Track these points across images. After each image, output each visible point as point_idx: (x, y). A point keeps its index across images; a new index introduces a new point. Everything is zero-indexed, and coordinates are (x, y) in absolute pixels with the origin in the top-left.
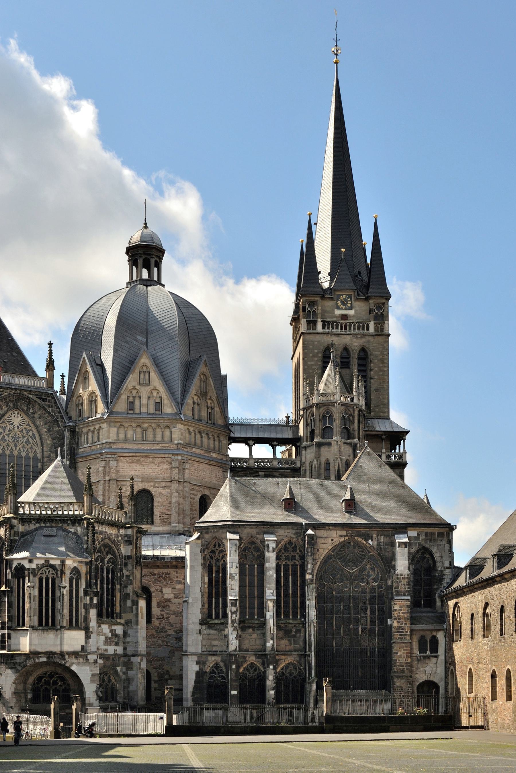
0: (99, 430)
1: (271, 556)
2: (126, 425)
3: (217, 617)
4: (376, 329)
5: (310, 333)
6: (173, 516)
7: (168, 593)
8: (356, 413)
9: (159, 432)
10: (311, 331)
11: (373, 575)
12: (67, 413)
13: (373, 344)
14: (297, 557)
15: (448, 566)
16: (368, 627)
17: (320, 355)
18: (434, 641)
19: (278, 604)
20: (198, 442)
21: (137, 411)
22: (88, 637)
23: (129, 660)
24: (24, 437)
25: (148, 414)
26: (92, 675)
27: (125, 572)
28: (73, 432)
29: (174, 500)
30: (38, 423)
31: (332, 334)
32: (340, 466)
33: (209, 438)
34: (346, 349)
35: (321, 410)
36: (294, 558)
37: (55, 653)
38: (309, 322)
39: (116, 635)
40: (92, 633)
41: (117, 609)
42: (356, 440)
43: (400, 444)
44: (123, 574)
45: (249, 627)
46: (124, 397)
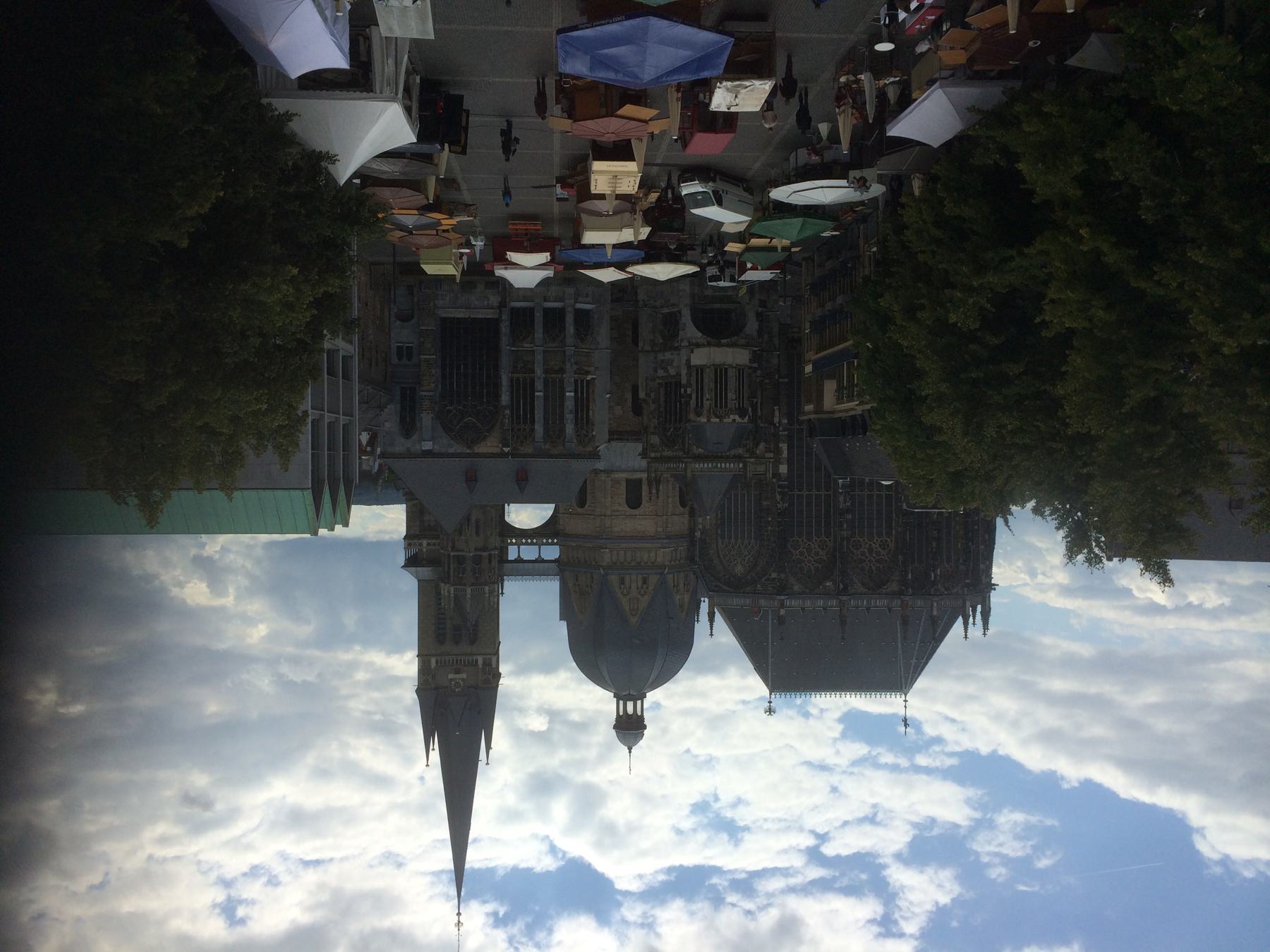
1: (539, 428)
3: (582, 381)
6: (610, 486)
7: (618, 411)
8: (452, 579)
9: (622, 560)
10: (489, 656)
12: (697, 578)
14: (516, 430)
15: (386, 424)
17: (480, 635)
18: (400, 357)
19: (533, 391)
21: (640, 576)
22: (688, 361)
23: (652, 348)
24: (733, 556)
25: (630, 574)
26: (685, 330)
27: (656, 421)
28: (692, 560)
29: (610, 499)
32: (466, 527)
33: (577, 558)
34: (457, 643)
35: (483, 580)
37: (714, 346)
38: (490, 665)
39: (663, 369)
40: (686, 364)
41: (662, 391)
42: (452, 554)
44: (657, 419)
46: (651, 588)
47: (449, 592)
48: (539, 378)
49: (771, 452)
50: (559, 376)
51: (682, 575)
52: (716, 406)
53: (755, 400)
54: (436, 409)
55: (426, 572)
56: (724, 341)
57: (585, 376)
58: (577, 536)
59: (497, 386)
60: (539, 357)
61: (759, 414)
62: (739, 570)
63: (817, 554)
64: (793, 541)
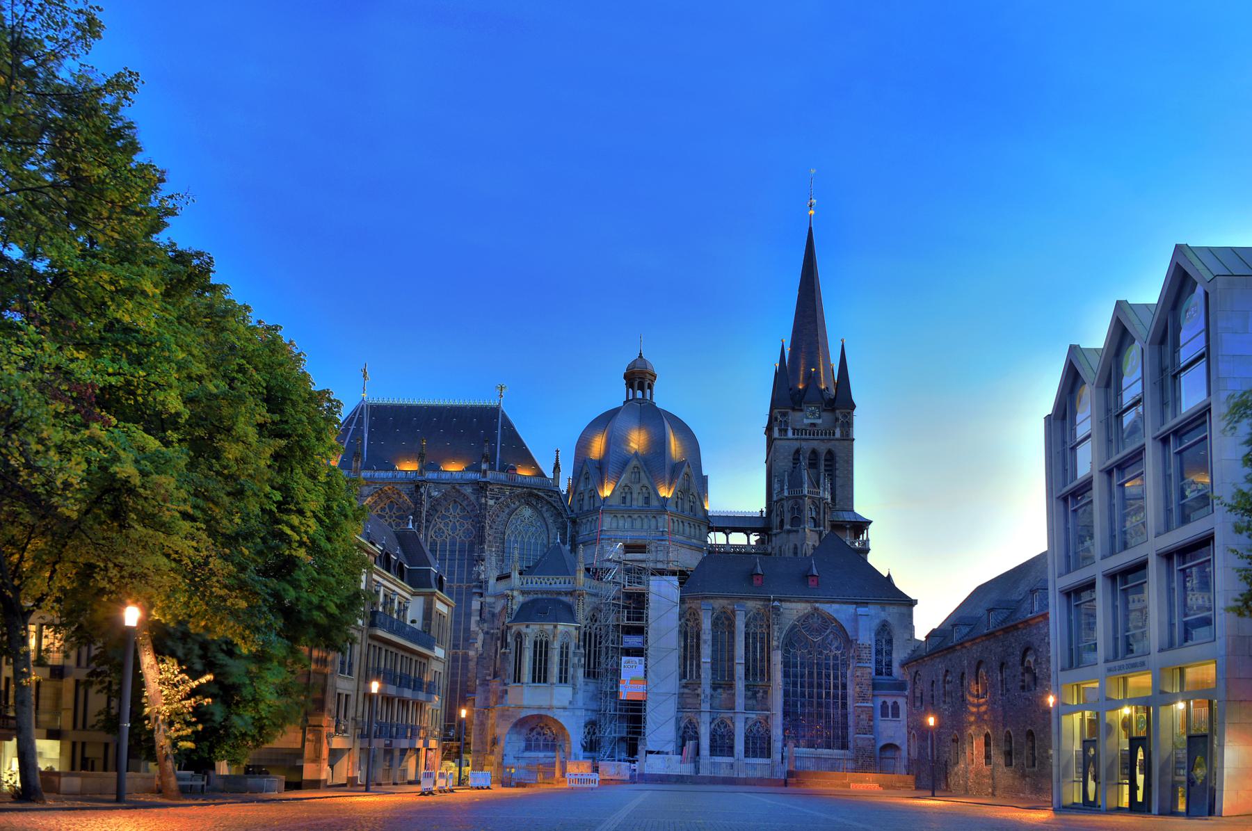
0: (596, 521)
2: (619, 516)
4: (842, 435)
5: (781, 439)
11: (836, 644)
13: (837, 447)
16: (832, 691)
17: (791, 458)
18: (896, 707)
20: (681, 530)
21: (628, 504)
22: (574, 694)
30: (545, 515)
31: (800, 439)
34: (814, 452)
36: (761, 626)
38: (780, 430)
42: (822, 528)
43: (863, 533)
45: (721, 687)
47: (824, 491)
48: (740, 678)
49: (489, 604)
50: (717, 682)
51: (585, 508)
52: (547, 643)
53: (503, 650)
54: (852, 651)
55: (847, 517)
56: (535, 712)
57: (690, 682)
58: (692, 547)
59: (786, 675)
60: (740, 702)
61: (499, 642)
62: (527, 512)
63: (446, 525)
64: (470, 537)
